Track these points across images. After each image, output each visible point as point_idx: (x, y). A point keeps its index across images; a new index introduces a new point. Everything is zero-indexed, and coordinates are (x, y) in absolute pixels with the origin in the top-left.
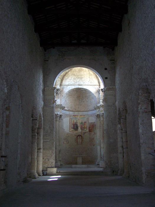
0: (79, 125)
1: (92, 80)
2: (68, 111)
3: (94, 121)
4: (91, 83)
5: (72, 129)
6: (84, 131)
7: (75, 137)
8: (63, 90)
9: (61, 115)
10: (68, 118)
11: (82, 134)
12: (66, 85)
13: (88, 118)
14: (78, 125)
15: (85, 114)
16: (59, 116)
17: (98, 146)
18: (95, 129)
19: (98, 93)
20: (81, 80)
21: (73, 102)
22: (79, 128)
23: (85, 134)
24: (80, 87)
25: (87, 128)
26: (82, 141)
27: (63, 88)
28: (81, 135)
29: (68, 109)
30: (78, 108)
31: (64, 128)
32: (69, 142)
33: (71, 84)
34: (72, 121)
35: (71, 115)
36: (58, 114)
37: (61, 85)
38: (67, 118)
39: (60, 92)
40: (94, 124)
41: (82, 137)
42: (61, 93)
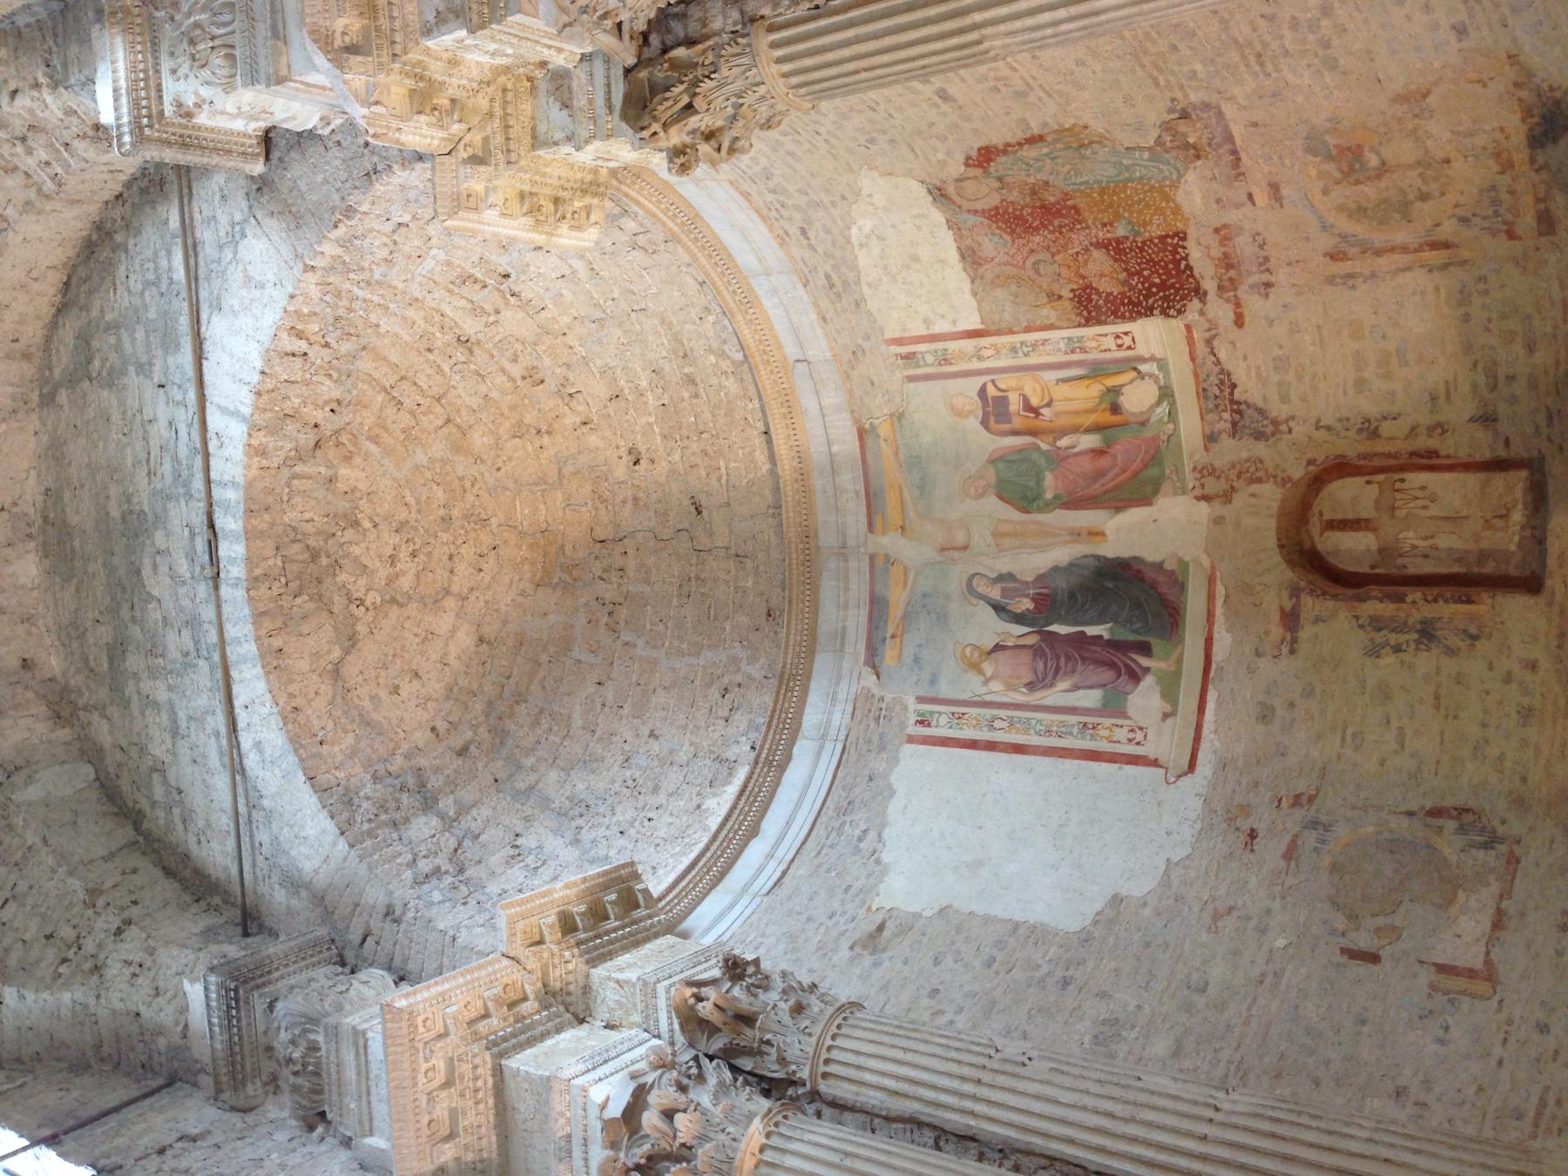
1: (140, 335)
3: (923, 191)
5: (1145, 700)
6: (1190, 425)
8: (308, 886)
13: (907, 351)
14: (1061, 554)
18: (1077, 140)
21: (654, 663)
23: (1249, 389)
25: (1097, 370)
26: (1428, 461)
27: (295, 884)
28: (1271, 495)
29: (742, 774)
31: (1073, 924)
34: (973, 686)
35: (869, 710)
38: (895, 807)
40: (985, 193)
41: (1341, 468)
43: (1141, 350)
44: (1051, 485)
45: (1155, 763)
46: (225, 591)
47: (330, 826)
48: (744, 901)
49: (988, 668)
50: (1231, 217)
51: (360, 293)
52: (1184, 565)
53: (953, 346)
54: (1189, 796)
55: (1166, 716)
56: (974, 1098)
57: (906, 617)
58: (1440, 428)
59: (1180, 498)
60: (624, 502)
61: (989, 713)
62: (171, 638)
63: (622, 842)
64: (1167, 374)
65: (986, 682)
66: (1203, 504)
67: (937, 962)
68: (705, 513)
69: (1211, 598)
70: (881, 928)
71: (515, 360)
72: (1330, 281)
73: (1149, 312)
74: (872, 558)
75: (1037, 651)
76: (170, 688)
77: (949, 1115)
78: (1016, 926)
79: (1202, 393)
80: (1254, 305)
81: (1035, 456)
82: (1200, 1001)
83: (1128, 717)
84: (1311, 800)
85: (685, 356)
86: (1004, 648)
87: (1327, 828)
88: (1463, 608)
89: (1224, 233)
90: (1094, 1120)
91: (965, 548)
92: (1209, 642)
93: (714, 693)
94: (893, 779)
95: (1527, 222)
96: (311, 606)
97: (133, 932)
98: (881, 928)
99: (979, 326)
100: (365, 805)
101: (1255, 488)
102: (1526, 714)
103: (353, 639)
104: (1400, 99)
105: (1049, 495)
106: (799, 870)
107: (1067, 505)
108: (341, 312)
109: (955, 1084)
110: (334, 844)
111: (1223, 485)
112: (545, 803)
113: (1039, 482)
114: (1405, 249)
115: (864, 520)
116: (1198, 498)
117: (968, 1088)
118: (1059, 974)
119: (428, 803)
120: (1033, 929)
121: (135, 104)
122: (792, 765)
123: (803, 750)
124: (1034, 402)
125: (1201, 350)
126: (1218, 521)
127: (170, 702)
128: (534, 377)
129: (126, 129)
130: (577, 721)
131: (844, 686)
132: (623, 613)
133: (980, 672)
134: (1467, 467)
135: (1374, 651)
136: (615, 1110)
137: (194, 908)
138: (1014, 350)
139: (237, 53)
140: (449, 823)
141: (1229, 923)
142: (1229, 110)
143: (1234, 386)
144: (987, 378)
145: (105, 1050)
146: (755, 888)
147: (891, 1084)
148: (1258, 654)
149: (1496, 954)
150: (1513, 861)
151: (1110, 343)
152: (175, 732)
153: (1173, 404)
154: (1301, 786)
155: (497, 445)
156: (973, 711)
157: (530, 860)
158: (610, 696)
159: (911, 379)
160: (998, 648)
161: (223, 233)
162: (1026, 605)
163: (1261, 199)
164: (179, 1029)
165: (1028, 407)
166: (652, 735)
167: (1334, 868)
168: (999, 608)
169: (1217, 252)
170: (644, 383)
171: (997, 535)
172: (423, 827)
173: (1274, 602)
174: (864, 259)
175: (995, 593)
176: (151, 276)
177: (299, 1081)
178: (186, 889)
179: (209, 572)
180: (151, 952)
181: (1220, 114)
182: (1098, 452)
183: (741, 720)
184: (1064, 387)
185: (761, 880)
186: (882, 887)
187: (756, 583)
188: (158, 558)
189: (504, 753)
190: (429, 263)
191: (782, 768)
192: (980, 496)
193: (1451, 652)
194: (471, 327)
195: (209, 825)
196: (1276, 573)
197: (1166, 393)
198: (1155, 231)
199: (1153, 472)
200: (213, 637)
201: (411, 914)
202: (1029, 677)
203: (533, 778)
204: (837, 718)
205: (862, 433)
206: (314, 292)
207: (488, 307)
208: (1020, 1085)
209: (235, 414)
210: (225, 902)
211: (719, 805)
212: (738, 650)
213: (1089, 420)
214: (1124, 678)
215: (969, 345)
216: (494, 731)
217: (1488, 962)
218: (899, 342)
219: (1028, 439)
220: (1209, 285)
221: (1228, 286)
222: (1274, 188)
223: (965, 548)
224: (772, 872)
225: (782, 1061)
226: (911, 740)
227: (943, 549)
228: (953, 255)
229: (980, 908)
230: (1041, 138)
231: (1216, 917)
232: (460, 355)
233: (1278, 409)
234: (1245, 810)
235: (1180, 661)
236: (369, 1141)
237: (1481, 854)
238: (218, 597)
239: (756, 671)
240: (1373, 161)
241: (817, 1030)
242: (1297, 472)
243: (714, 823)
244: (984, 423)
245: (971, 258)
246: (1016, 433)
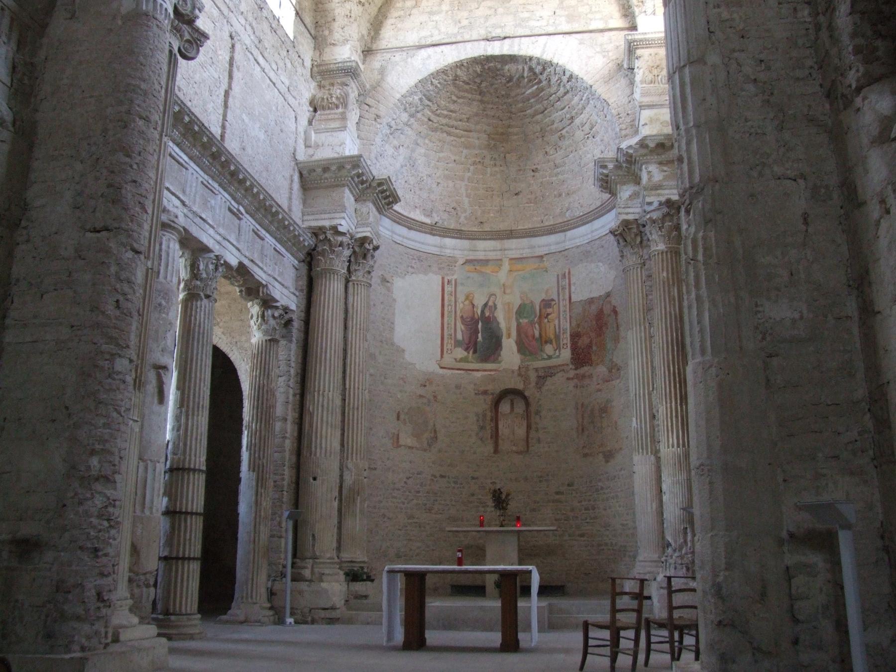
0: (504, 321)
2: (433, 230)
4: (570, 18)
5: (460, 353)
7: (484, 404)
8: (382, 79)
9: (363, 241)
10: (434, 281)
11: (526, 379)
12: (401, 49)
13: (566, 276)
14: (503, 325)
15: (543, 251)
16: (345, 239)
17: (636, 458)
18: (616, 340)
19: (623, 82)
20: (500, 10)
21: (463, 180)
22: (509, 345)
23: (549, 381)
24: (496, 49)
25: (557, 337)
26: (529, 427)
27: (382, 71)
28: (520, 386)
29: (427, 221)
30: (500, 211)
31: (396, 341)
32: (436, 438)
33: (436, 39)
34: (461, 298)
35: (452, 261)
36: (335, 230)
37: (367, 52)
38: (421, 276)
39: (363, 94)
40: (607, 310)
41: (528, 404)
42: (369, 101)
43: (563, 351)
44: (524, 321)
45: (442, 356)
46: (483, 43)
47: (404, 91)
48: (390, 233)
49: (467, 302)
50: (595, 379)
51: (585, 95)
52: (500, 362)
53: (567, 291)
54: (433, 367)
55: (456, 359)
56: (356, 329)
57: (482, 272)
58: (537, 430)
59: (519, 361)
60: (519, 166)
61: (453, 303)
62: (465, 14)
63: (403, 183)
64: (555, 358)
65: (463, 303)
66: (516, 368)
67: (382, 303)
68: (516, 197)
69: (491, 370)
70: (388, 282)
71: (567, 132)
72: (577, 403)
73: (573, 354)
74: (501, 260)
75: (473, 318)
76: (447, 12)
77: (351, 323)
78: (393, 323)
79: (550, 367)
80: (572, 384)
81: (533, 317)
82: (383, 378)
83: (455, 347)
84: (436, 401)
85: (568, 194)
86: (473, 307)
87: (428, 405)
88: (489, 436)
89: (591, 376)
90: (357, 360)
91: (505, 293)
92: (478, 370)
93: (454, 205)
94: (431, 274)
95: (586, 451)
96: (479, 72)
97: (360, 8)
98: (388, 282)
99: (572, 301)
100: (411, 99)
101: (522, 382)
102: (463, 452)
103: (468, 84)
104: (616, 422)
105: (521, 321)
106: (401, 248)
107: (518, 326)
108: (579, 89)
109: (359, 323)
110: (398, 92)
111: (523, 373)
112: (413, 151)
113: (525, 317)
114: (583, 422)
115: (513, 256)
116: (520, 368)
117: (358, 326)
118: (384, 339)
119: (412, 116)
120: (393, 329)
121: (641, 40)
122: (432, 237)
123: (436, 240)
124: (549, 317)
125: (561, 368)
126: (513, 372)
127: (442, 11)
128: (561, 138)
129: (633, 37)
130: (441, 155)
131: (460, 252)
132: (480, 166)
133: (466, 300)
134: (528, 437)
135: (477, 415)
136: (340, 229)
137: (368, 25)
138: (565, 311)
139: (652, 85)
140: (406, 124)
141: (401, 382)
142: (618, 381)
143: (551, 377)
144: (557, 301)
145: (320, 6)
146: (395, 236)
147: (355, 304)
148: (475, 384)
149: (402, 447)
150: (425, 450)
151: (565, 341)
152: (431, 13)
153: (547, 359)
154: (439, 397)
155: (537, 123)
156: (453, 299)
157: (396, 153)
158: (450, 165)
159: (558, 275)
160: (473, 306)
161: (605, 46)
162: (487, 314)
163: (598, 387)
164: (333, 42)
165: (548, 315)
166: (438, 183)
167: (419, 408)
168: (486, 305)
169: (587, 374)
170: (560, 177)
171: (509, 304)
172: (405, 117)
173: (490, 387)
174: (593, 265)
175: (490, 303)
176: (594, 9)
177: (326, 100)
178: (375, 18)
179: (490, 36)
180: (355, 20)
181: (617, 378)
182: (534, 336)
183: (445, 216)
184: (552, 327)
185: (397, 237)
186: (398, 278)
187: (492, 217)
188: (493, 10)
189: (430, 132)
190: (596, 118)
191: (431, 234)
192: (521, 298)
193: (477, 434)
194: (577, 121)
195: (399, 30)
196: (498, 388)
197: (550, 357)
198: (593, 357)
199: (527, 353)
200: (467, 37)
201: (378, 126)
202: (465, 317)
203: (422, 145)
204: (448, 251)
205: (542, 257)
206: (585, 85)
207: (584, 128)
208: (361, 341)
209: (543, 52)
210: (372, 38)
211: (418, 216)
212: (469, 212)
213: (543, 335)
214: (466, 346)
215: (567, 297)
216: (437, 128)
217: (401, 446)
218: (569, 273)
219: (538, 314)
220: (578, 372)
221: (577, 376)
222: (599, 390)
223: (505, 293)
224: (398, 239)
225: (356, 270)
226: (443, 278)
227: (504, 285)
228: (592, 295)
229: (396, 311)
230: (618, 329)
231: (402, 379)
232: (568, 116)
233: (545, 388)
234: (431, 383)
235: (472, 362)
236: (313, 132)
237: (426, 442)
238: (480, 40)
239: (462, 219)
240: (603, 415)
241: (365, 280)
242: (526, 394)
243: (412, 216)
244: (543, 300)
245: (591, 301)
246: (540, 310)
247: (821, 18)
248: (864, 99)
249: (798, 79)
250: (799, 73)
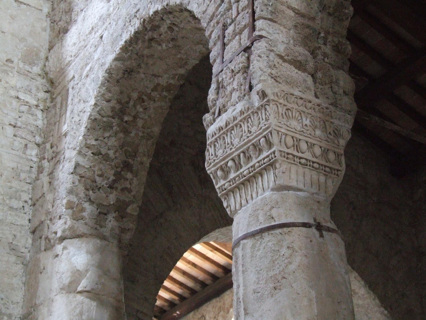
247: (46, 163)
248: (65, 248)
249: (11, 208)
250: (15, 204)
